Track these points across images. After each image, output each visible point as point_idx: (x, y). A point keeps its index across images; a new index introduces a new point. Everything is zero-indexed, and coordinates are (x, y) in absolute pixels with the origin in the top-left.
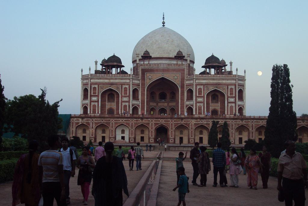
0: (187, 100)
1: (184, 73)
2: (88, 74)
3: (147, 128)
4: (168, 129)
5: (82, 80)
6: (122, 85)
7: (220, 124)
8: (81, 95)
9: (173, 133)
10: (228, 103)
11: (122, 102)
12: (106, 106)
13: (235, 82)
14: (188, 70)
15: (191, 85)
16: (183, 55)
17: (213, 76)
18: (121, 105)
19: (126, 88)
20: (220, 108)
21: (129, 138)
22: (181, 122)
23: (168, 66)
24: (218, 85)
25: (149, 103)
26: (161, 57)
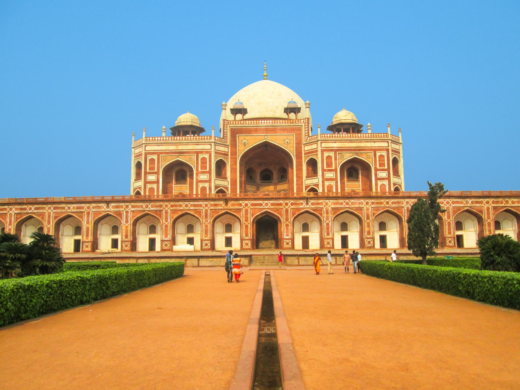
0: (307, 177)
3: (237, 220)
4: (280, 220)
5: (133, 150)
6: (197, 153)
9: (290, 227)
10: (377, 179)
11: (198, 182)
15: (312, 152)
17: (350, 136)
18: (197, 186)
19: (204, 159)
20: (363, 190)
21: (202, 241)
22: (304, 206)
24: (359, 150)
25: (245, 187)
26: (263, 117)
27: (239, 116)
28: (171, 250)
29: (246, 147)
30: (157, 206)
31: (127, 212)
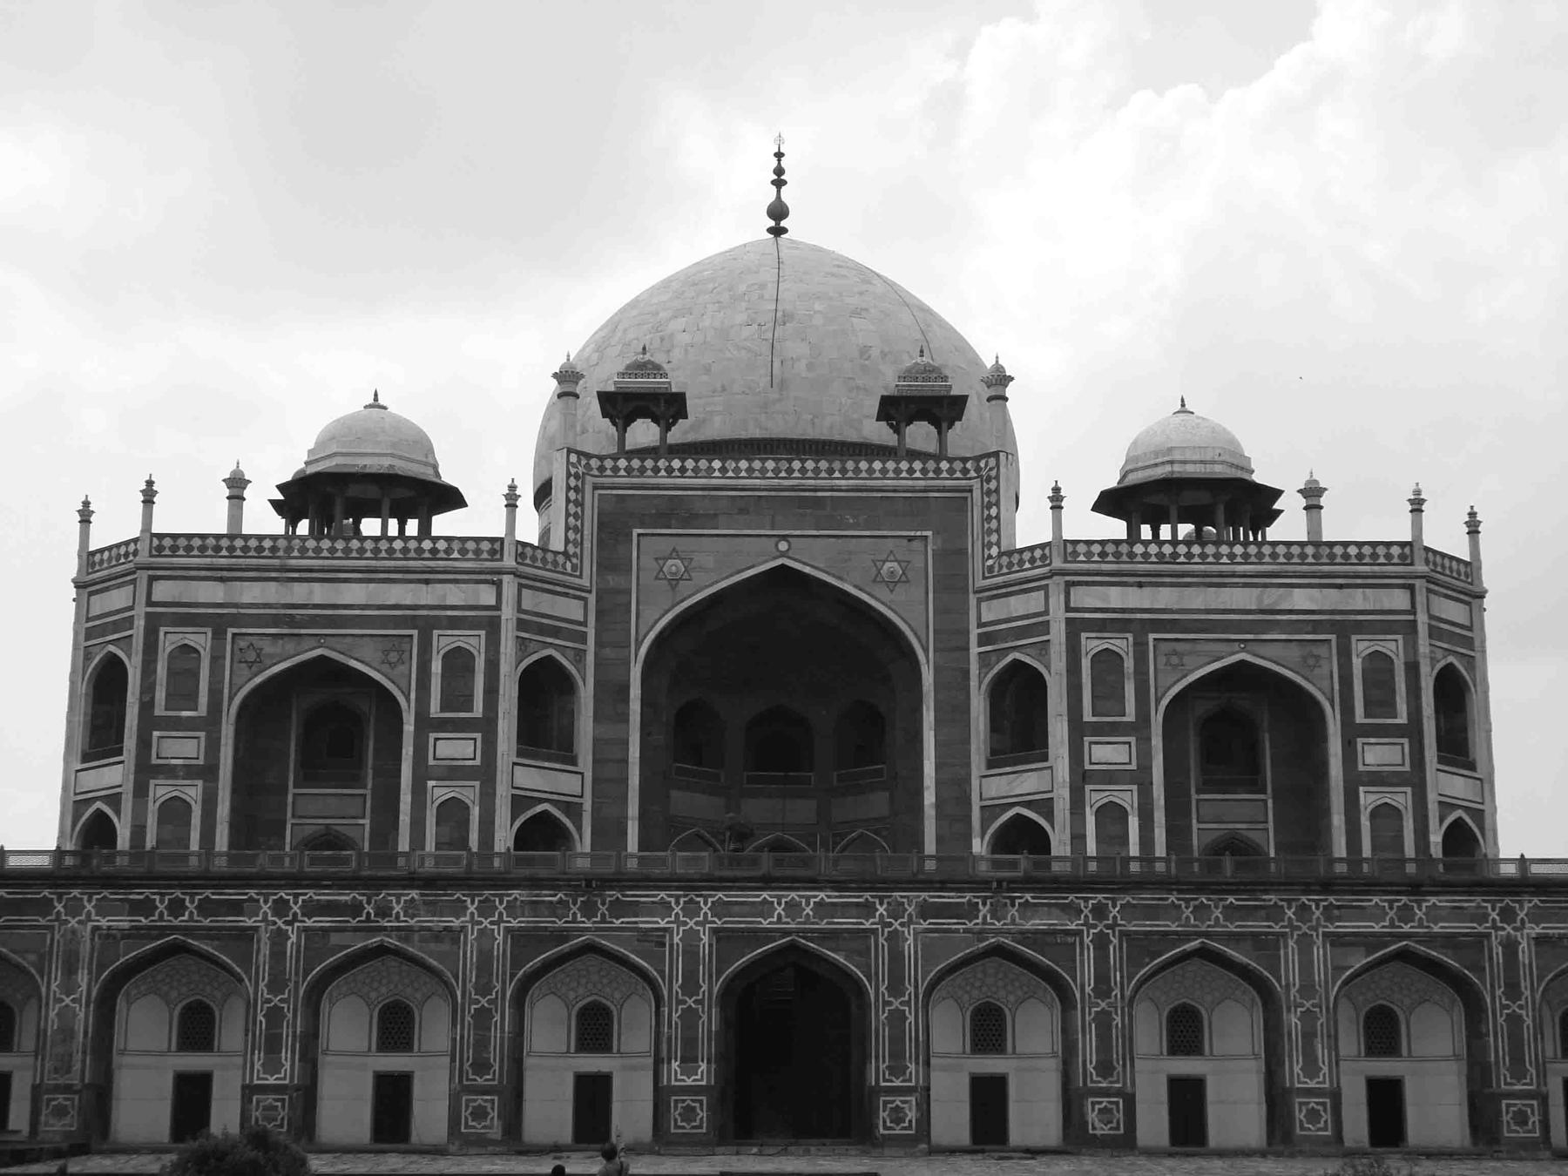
2: (135, 541)
4: (861, 991)
6: (426, 623)
11: (422, 774)
13: (1406, 605)
16: (954, 392)
23: (831, 471)
27: (643, 432)
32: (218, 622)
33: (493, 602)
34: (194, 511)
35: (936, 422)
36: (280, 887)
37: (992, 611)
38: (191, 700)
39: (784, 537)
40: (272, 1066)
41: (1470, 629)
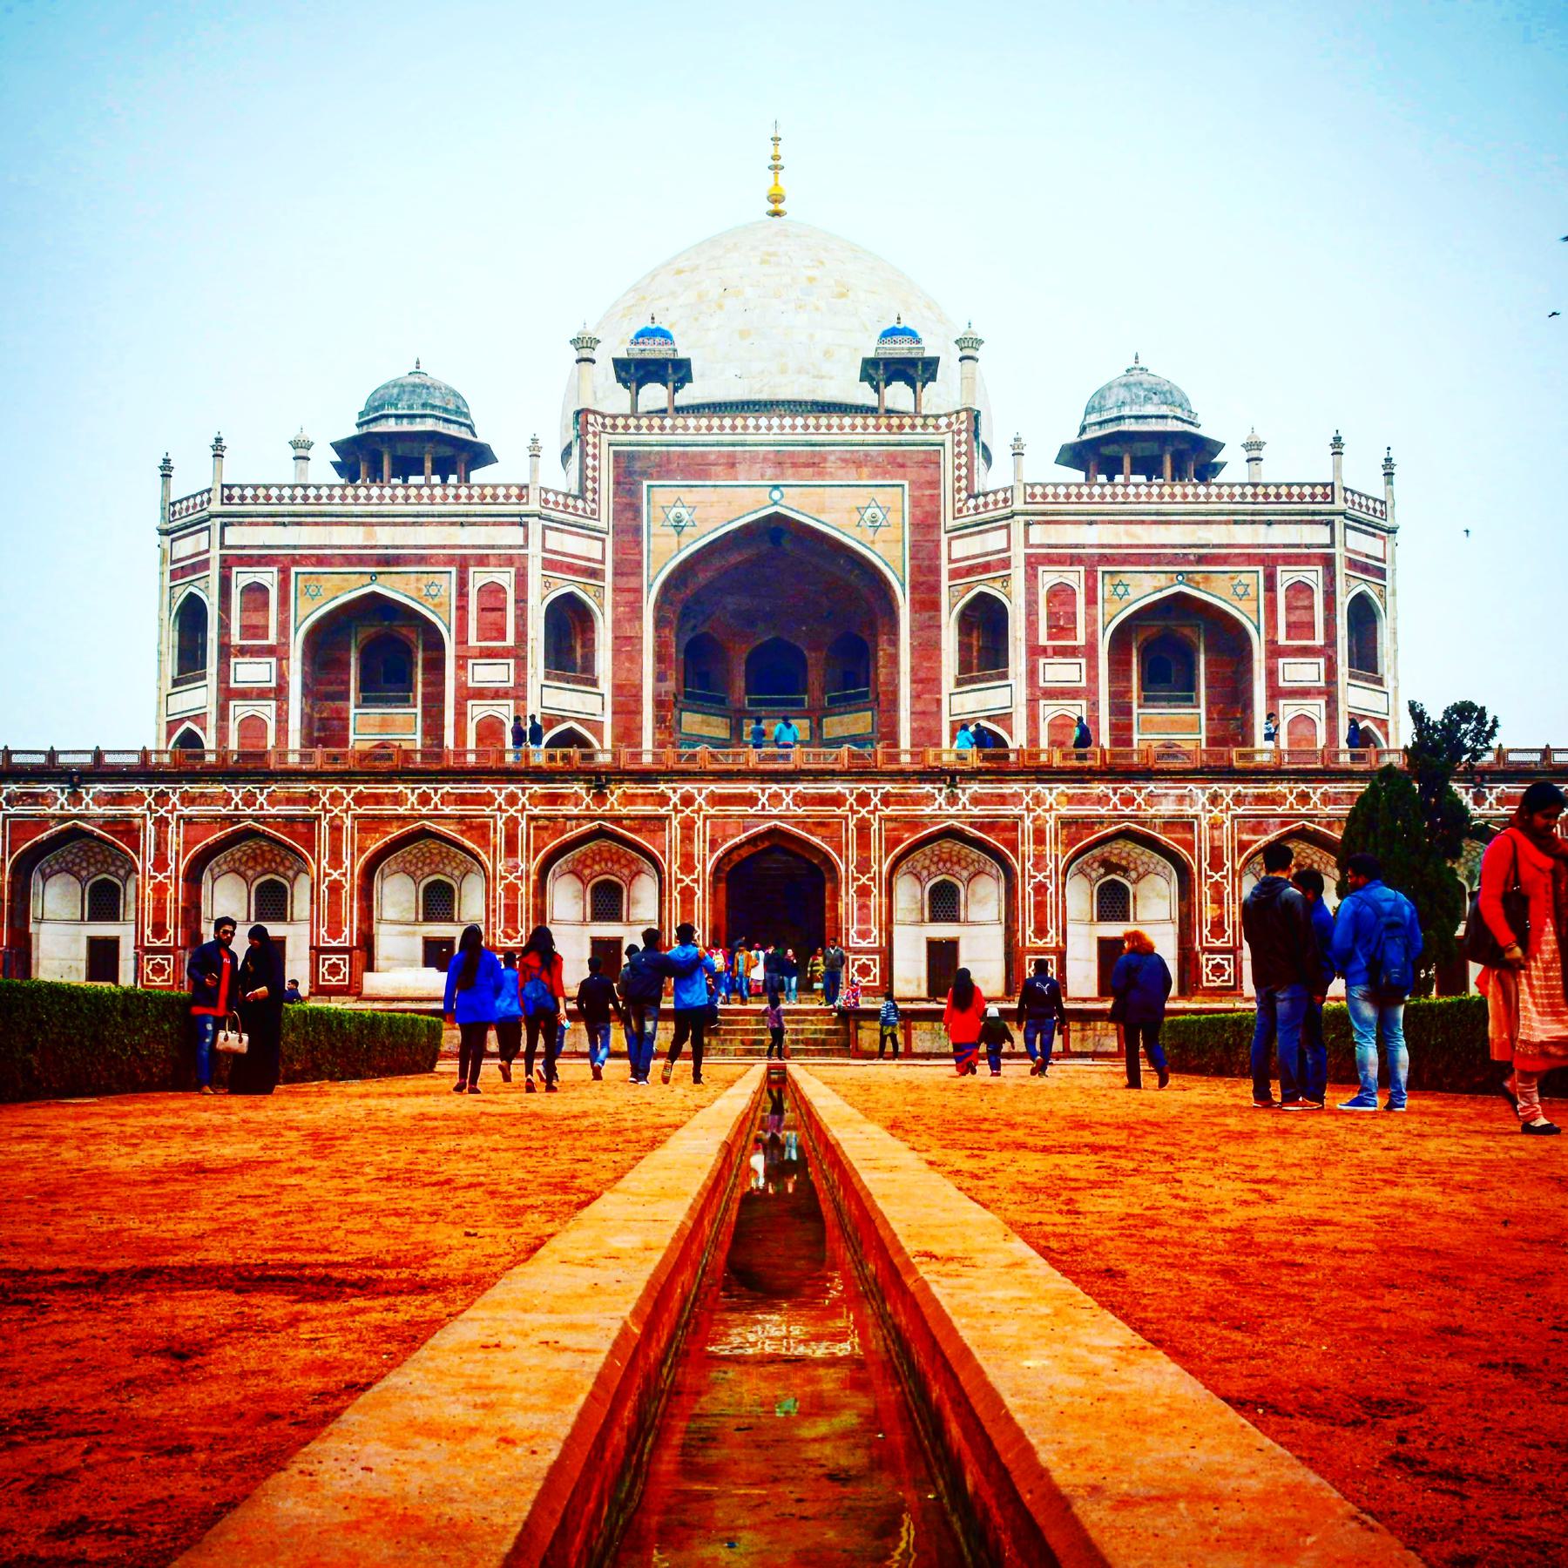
0: (959, 683)
1: (934, 484)
2: (209, 491)
3: (647, 865)
4: (833, 868)
5: (167, 539)
6: (463, 564)
7: (1285, 820)
8: (160, 653)
9: (876, 900)
10: (1275, 693)
12: (346, 728)
13: (1328, 541)
14: (964, 460)
15: (986, 568)
16: (927, 354)
17: (1161, 496)
18: (461, 714)
22: (941, 807)
24: (1201, 559)
25: (679, 722)
26: (764, 396)
27: (654, 395)
28: (353, 989)
29: (685, 540)
30: (290, 800)
31: (162, 823)
32: (285, 563)
33: (521, 542)
34: (261, 462)
35: (911, 383)
36: (335, 782)
37: (966, 548)
38: (262, 632)
39: (776, 487)
40: (335, 932)
41: (1384, 561)
